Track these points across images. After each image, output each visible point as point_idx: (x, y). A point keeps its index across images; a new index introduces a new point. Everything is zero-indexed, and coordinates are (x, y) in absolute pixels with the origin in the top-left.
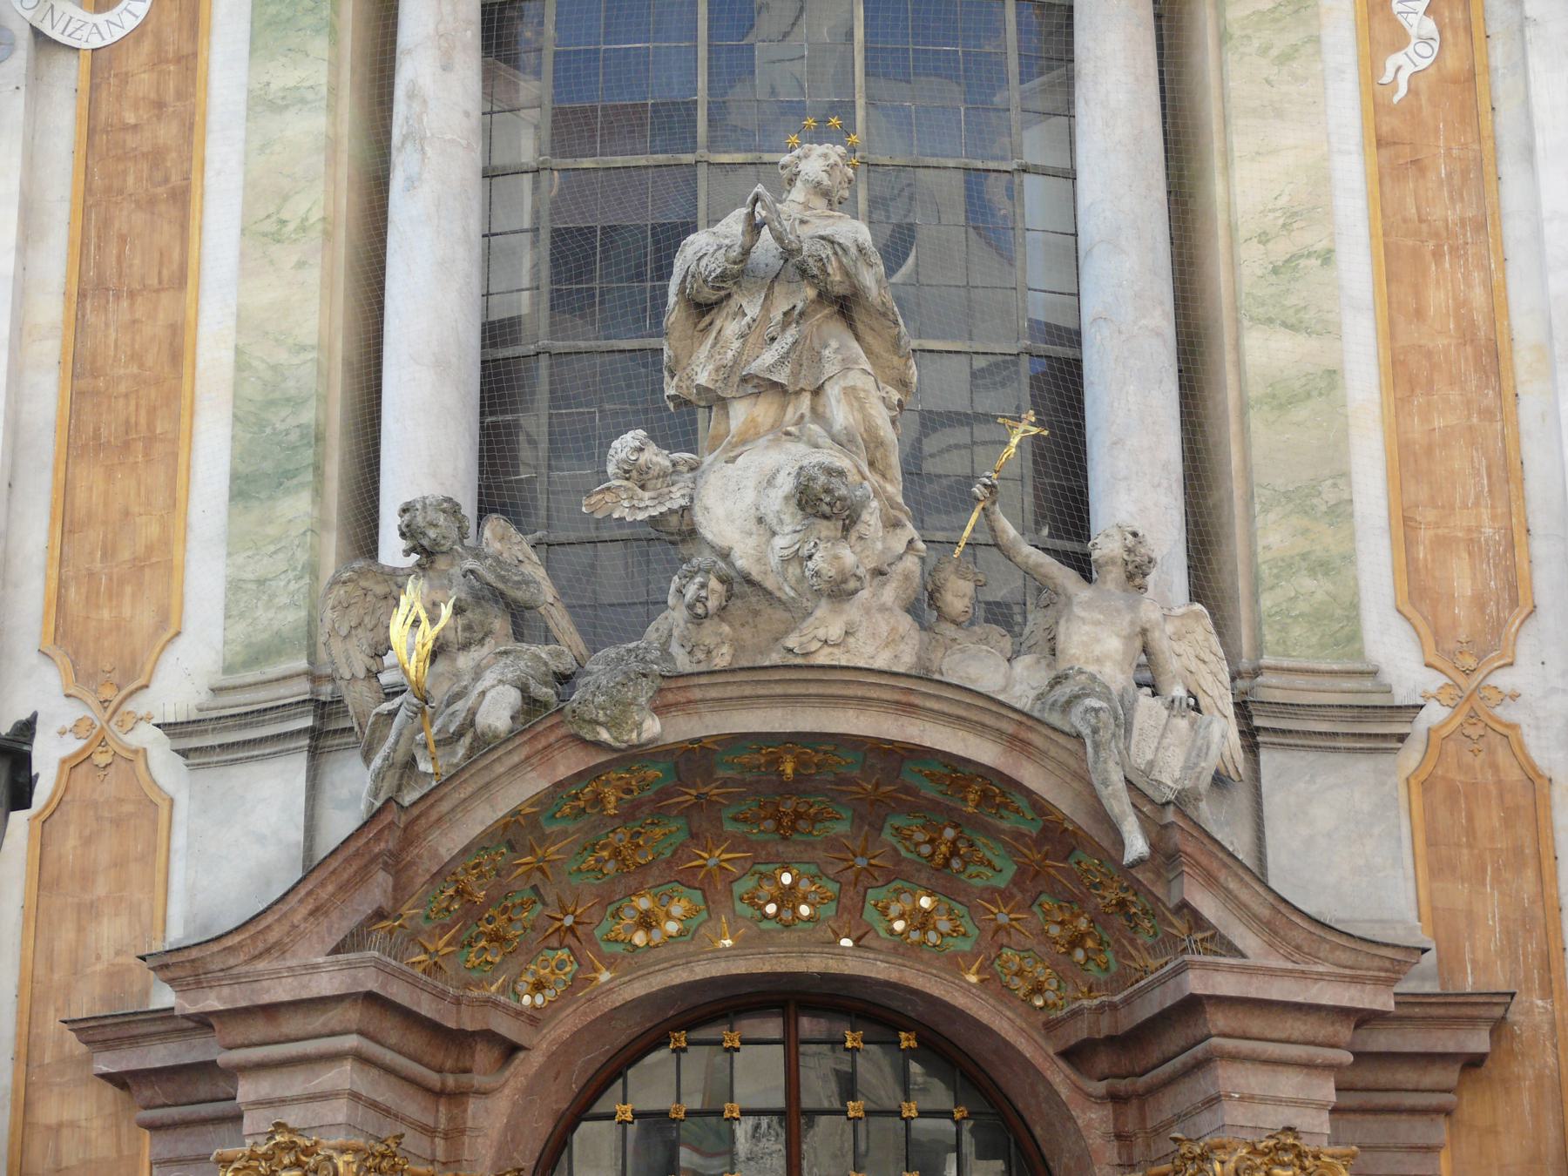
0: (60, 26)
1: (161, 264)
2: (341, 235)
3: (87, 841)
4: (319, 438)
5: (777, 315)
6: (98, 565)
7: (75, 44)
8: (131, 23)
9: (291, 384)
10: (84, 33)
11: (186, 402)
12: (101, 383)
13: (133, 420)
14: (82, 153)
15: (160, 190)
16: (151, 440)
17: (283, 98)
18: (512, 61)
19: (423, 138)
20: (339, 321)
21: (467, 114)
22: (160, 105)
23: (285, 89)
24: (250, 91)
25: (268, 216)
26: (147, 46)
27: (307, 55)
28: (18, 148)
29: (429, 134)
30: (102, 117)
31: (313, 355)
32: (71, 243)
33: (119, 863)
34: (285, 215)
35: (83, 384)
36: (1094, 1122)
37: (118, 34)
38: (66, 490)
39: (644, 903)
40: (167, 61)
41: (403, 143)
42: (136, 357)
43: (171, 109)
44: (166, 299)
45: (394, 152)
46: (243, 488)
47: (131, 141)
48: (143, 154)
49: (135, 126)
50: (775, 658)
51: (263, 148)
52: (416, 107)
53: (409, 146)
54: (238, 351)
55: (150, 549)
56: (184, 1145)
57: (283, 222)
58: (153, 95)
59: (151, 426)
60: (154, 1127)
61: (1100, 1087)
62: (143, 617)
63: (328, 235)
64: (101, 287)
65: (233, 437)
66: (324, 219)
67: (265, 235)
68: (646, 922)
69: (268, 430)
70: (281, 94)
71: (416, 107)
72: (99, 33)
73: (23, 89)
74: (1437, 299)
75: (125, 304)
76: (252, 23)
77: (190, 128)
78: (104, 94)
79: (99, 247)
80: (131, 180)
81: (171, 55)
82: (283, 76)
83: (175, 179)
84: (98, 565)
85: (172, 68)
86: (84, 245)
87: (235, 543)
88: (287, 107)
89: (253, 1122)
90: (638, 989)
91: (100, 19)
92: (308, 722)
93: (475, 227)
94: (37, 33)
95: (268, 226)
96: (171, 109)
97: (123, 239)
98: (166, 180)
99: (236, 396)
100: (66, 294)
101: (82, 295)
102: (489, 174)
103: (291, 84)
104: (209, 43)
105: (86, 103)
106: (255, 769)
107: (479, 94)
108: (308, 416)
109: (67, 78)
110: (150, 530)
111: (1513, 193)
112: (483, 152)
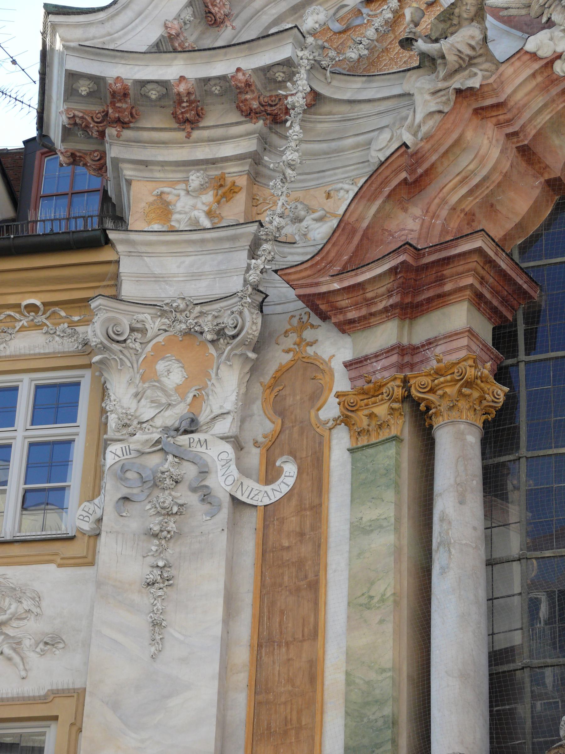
0: (247, 494)
1: (303, 626)
2: (405, 603)
4: (395, 723)
7: (255, 503)
8: (285, 489)
9: (377, 691)
10: (260, 496)
11: (318, 705)
12: (271, 697)
13: (289, 717)
14: (259, 564)
15: (302, 583)
16: (300, 728)
17: (370, 526)
18: (504, 497)
19: (449, 544)
20: (404, 653)
21: (475, 529)
22: (302, 534)
23: (371, 521)
24: (351, 523)
25: (363, 594)
26: (294, 502)
27: (383, 501)
28: (223, 563)
29: (452, 541)
30: (270, 543)
31: (390, 674)
32: (254, 616)
34: (372, 593)
35: (260, 698)
37: (279, 496)
40: (305, 510)
41: (438, 547)
42: (290, 681)
43: (308, 536)
44: (306, 645)
45: (434, 553)
47: (286, 556)
48: (293, 563)
49: (288, 548)
51: (359, 555)
52: (445, 526)
53: (441, 549)
54: (348, 674)
57: (371, 597)
58: (298, 529)
59: (299, 720)
63: (396, 603)
64: (271, 640)
65: (346, 725)
66: (394, 594)
67: (361, 605)
69: (365, 720)
70: (369, 524)
71: (445, 526)
72: (268, 496)
73: (226, 530)
75: (284, 650)
76: (352, 484)
78: (271, 530)
79: (269, 618)
80: (286, 578)
81: (307, 506)
83: (311, 576)
85: (308, 513)
86: (261, 617)
88: (372, 531)
91: (268, 488)
93: (482, 594)
94: (234, 499)
95: (363, 600)
96: (308, 536)
97: (282, 612)
98: (306, 577)
99: (347, 701)
100: (251, 646)
101: (260, 646)
102: (490, 563)
103: (374, 517)
104: (328, 498)
105: (261, 535)
107: (483, 517)
108: (387, 710)
112: (486, 548)
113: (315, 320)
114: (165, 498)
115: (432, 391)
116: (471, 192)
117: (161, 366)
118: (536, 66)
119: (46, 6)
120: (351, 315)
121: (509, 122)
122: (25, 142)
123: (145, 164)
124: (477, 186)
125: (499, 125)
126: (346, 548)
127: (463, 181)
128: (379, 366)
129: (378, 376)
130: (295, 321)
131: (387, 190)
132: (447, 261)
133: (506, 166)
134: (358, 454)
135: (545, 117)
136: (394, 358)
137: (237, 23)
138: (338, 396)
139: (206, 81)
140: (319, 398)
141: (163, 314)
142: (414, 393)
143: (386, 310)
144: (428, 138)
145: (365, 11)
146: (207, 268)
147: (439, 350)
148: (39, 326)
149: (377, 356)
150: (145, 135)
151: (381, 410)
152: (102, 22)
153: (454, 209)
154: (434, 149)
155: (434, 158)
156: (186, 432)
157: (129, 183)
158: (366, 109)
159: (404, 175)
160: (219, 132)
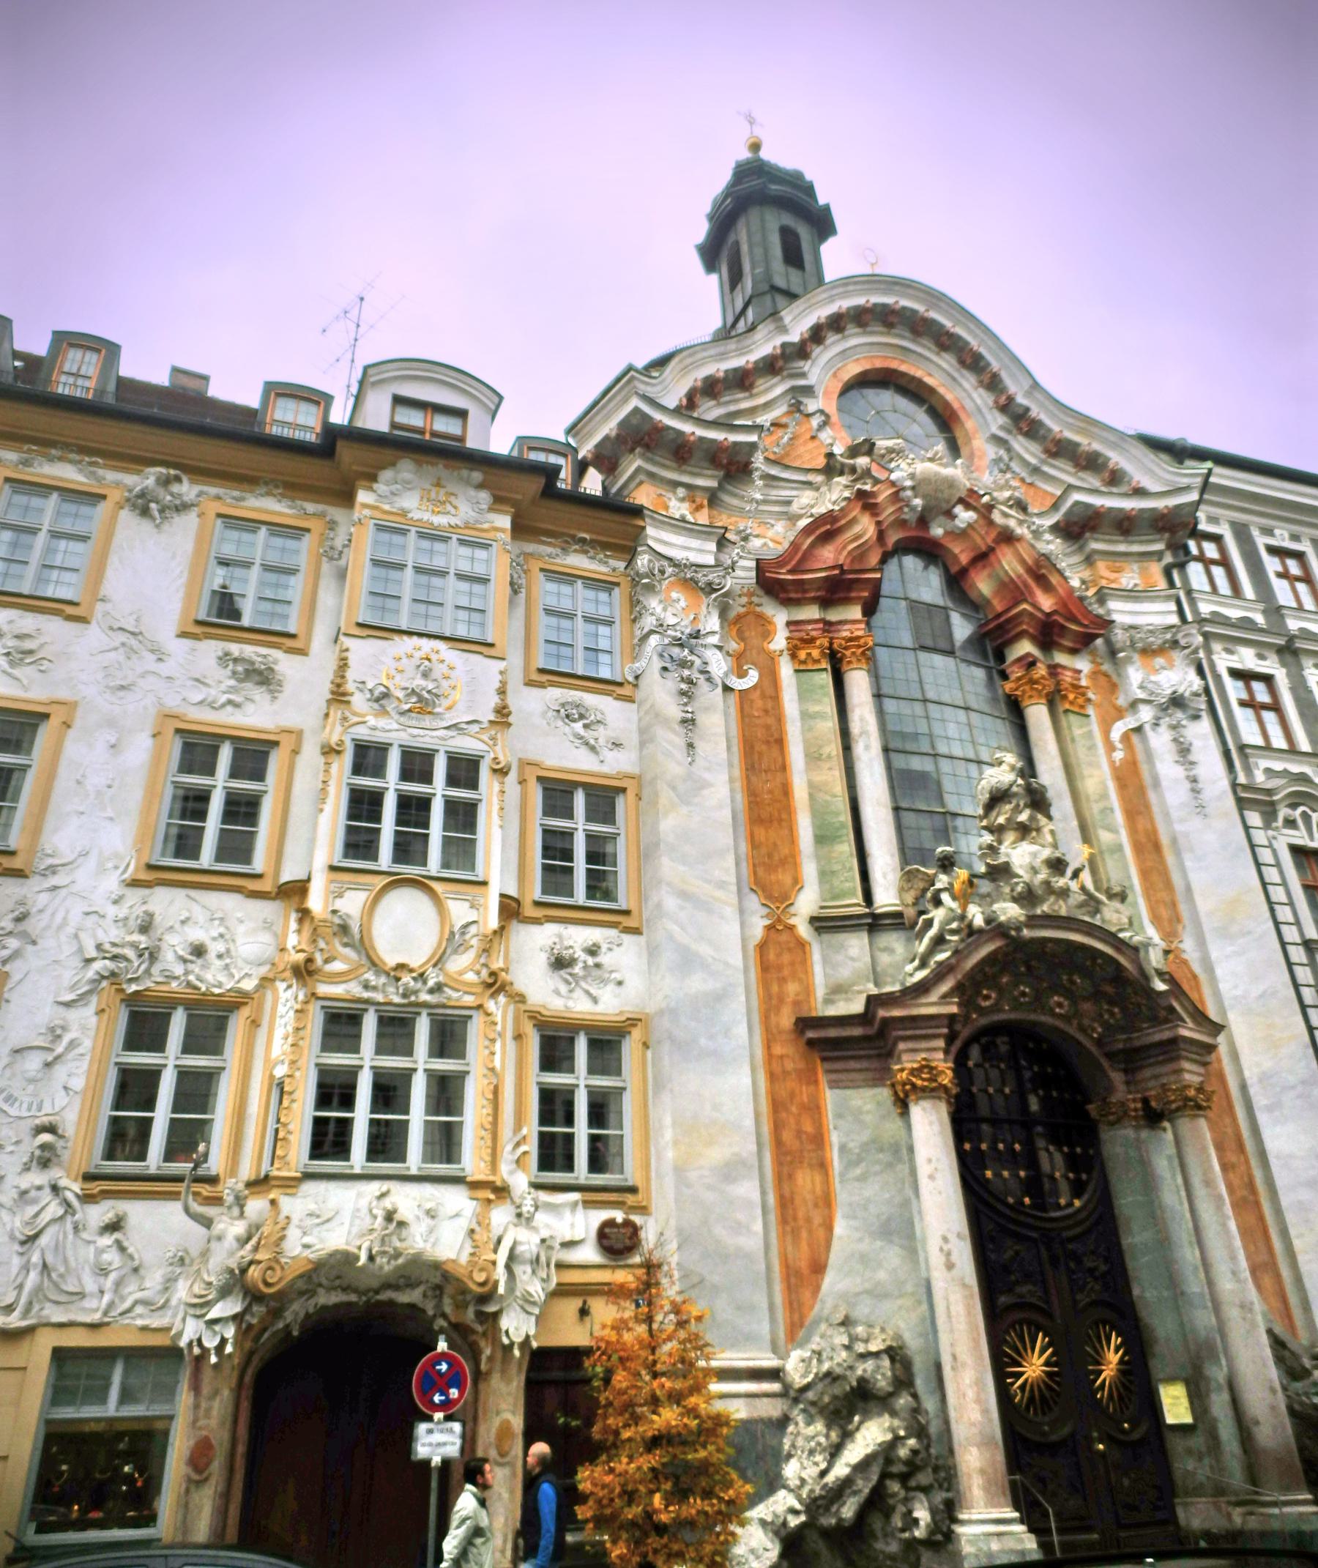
3: (779, 955)
8: (751, 684)
16: (780, 820)
26: (758, 692)
33: (792, 964)
38: (752, 835)
47: (758, 721)
50: (1039, 912)
55: (786, 858)
60: (824, 1059)
62: (787, 879)
64: (753, 767)
74: (1140, 827)
77: (780, 719)
87: (818, 858)
89: (905, 1057)
90: (984, 1021)
92: (869, 921)
109: (733, 699)
110: (785, 851)
111: (1152, 797)
113: (760, 592)
114: (686, 673)
115: (846, 648)
116: (858, 547)
117: (674, 595)
118: (894, 489)
120: (793, 595)
123: (652, 475)
125: (874, 514)
126: (799, 724)
128: (810, 627)
129: (814, 633)
130: (745, 590)
131: (818, 532)
132: (858, 580)
135: (892, 518)
136: (821, 626)
139: (701, 439)
141: (675, 565)
142: (835, 646)
144: (842, 510)
147: (846, 627)
148: (586, 552)
150: (658, 459)
151: (816, 653)
153: (850, 553)
154: (844, 517)
155: (843, 522)
156: (696, 638)
157: (641, 483)
158: (782, 484)
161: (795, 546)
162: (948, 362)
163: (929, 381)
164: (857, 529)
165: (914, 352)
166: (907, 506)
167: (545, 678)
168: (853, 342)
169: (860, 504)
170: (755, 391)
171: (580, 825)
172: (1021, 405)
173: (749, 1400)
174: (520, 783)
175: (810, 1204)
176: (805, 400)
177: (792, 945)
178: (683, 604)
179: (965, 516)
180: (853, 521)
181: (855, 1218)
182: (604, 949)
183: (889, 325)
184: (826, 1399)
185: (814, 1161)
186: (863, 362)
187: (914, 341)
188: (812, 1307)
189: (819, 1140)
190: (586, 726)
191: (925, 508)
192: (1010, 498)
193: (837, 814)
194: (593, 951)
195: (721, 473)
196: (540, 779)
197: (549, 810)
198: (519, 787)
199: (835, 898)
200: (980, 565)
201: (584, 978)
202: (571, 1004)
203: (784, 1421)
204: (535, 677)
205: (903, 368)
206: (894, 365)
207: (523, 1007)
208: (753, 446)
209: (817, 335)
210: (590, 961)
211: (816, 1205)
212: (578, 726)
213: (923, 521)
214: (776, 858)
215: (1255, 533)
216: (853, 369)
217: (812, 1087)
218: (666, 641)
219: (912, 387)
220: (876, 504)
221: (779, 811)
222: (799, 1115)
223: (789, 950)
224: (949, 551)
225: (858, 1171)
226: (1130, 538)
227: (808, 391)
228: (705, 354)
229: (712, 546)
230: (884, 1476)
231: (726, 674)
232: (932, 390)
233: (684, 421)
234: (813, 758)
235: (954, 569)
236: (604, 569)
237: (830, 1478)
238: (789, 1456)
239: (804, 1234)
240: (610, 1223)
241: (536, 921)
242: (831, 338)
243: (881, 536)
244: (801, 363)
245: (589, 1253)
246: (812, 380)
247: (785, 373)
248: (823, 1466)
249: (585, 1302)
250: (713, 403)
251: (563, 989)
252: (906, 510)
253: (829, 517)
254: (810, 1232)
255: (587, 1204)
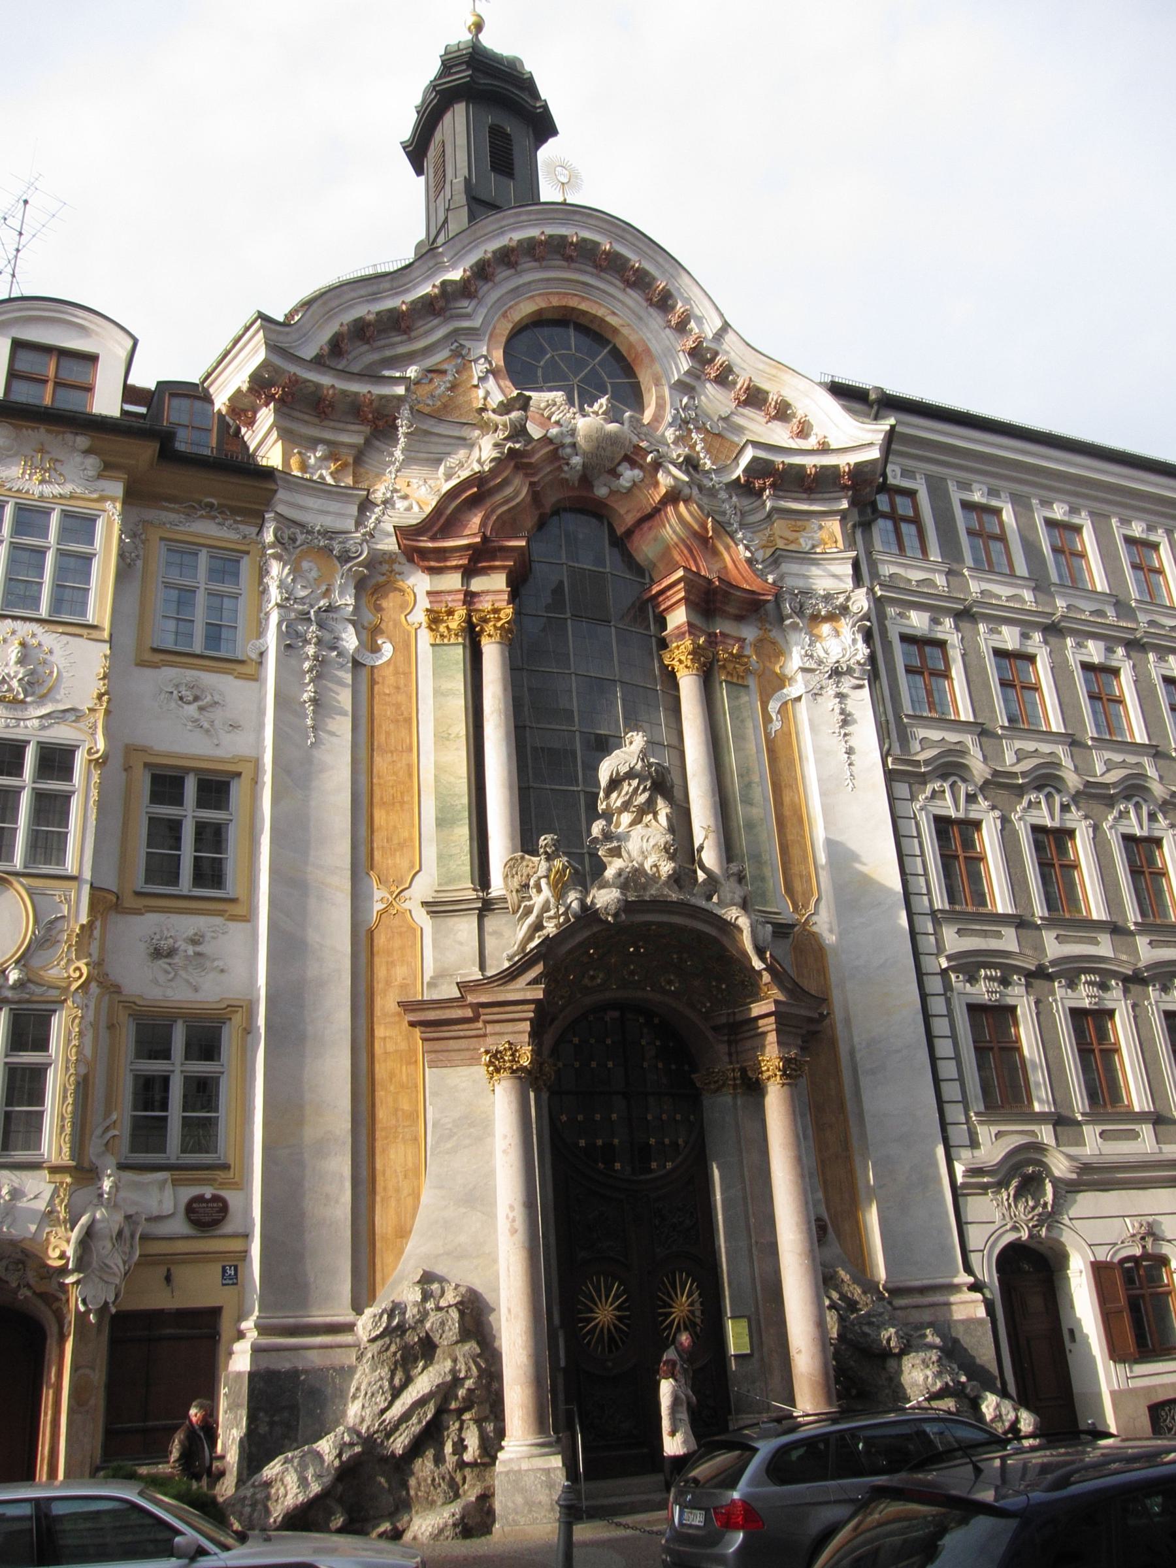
5: (642, 787)
6: (385, 844)
26: (391, 668)
33: (402, 948)
36: (723, 1048)
39: (591, 973)
42: (395, 774)
44: (405, 754)
46: (442, 822)
55: (405, 840)
56: (438, 1045)
61: (726, 1038)
62: (405, 864)
68: (593, 978)
82: (446, 685)
83: (406, 714)
84: (385, 844)
92: (480, 905)
106: (456, 919)
113: (403, 559)
116: (509, 510)
118: (551, 447)
119: (259, 312)
121: (533, 475)
122: (159, 383)
124: (513, 507)
125: (527, 475)
126: (431, 702)
127: (507, 501)
133: (529, 499)
134: (437, 648)
137: (350, 357)
138: (427, 610)
140: (405, 609)
143: (456, 568)
144: (491, 470)
145: (430, 376)
146: (331, 509)
148: (214, 518)
149: (449, 592)
152: (288, 334)
159: (475, 489)
160: (341, 425)
161: (438, 511)
162: (634, 300)
163: (611, 319)
164: (509, 491)
165: (598, 289)
166: (568, 464)
167: (158, 657)
168: (527, 278)
169: (512, 464)
170: (413, 334)
171: (189, 813)
172: (708, 349)
173: (321, 1351)
174: (126, 770)
175: (401, 1177)
176: (467, 344)
177: (404, 929)
178: (314, 574)
179: (629, 475)
180: (506, 482)
181: (442, 1187)
182: (209, 935)
183: (569, 259)
184: (393, 1348)
185: (408, 1137)
186: (538, 299)
187: (598, 277)
188: (394, 1268)
189: (413, 1116)
190: (201, 709)
191: (584, 466)
192: (679, 456)
193: (460, 797)
194: (195, 941)
195: (367, 429)
196: (147, 765)
197: (157, 797)
198: (124, 775)
199: (447, 884)
200: (646, 526)
201: (185, 968)
202: (169, 993)
203: (352, 1370)
204: (148, 656)
205: (583, 306)
206: (573, 303)
207: (117, 998)
208: (400, 399)
209: (482, 272)
210: (191, 950)
211: (406, 1177)
212: (191, 710)
213: (586, 480)
214: (395, 841)
215: (952, 487)
216: (526, 308)
217: (412, 1067)
218: (293, 615)
219: (595, 327)
220: (529, 465)
221: (402, 794)
222: (397, 1093)
223: (401, 934)
224: (612, 508)
225: (449, 1145)
226: (812, 496)
227: (473, 333)
228: (354, 295)
229: (353, 510)
230: (441, 1411)
231: (357, 650)
232: (615, 331)
233: (324, 374)
234: (441, 738)
235: (620, 531)
236: (233, 536)
237: (388, 1415)
238: (355, 1397)
239: (393, 1203)
240: (200, 1199)
241: (137, 912)
242: (502, 273)
243: (536, 496)
244: (465, 303)
245: (179, 1225)
246: (477, 323)
247: (448, 314)
248: (383, 1405)
249: (169, 1270)
250: (366, 347)
251: (162, 978)
252: (566, 468)
253: (478, 480)
254: (398, 1200)
255: (176, 1183)
